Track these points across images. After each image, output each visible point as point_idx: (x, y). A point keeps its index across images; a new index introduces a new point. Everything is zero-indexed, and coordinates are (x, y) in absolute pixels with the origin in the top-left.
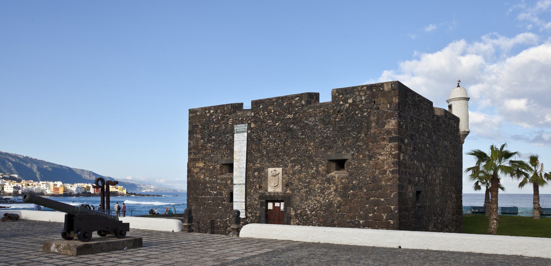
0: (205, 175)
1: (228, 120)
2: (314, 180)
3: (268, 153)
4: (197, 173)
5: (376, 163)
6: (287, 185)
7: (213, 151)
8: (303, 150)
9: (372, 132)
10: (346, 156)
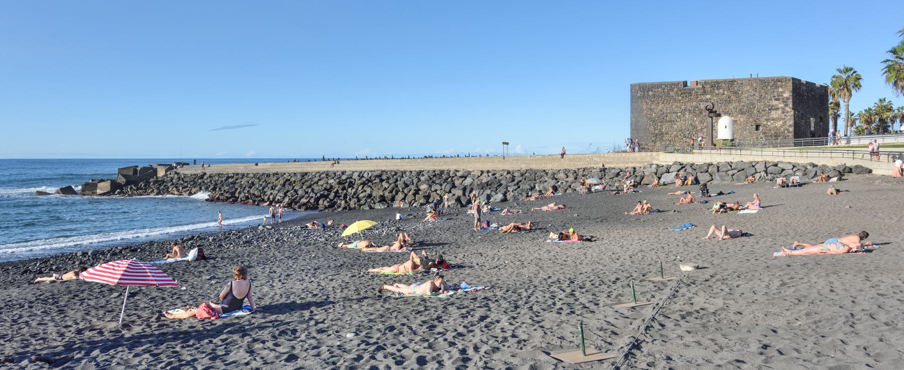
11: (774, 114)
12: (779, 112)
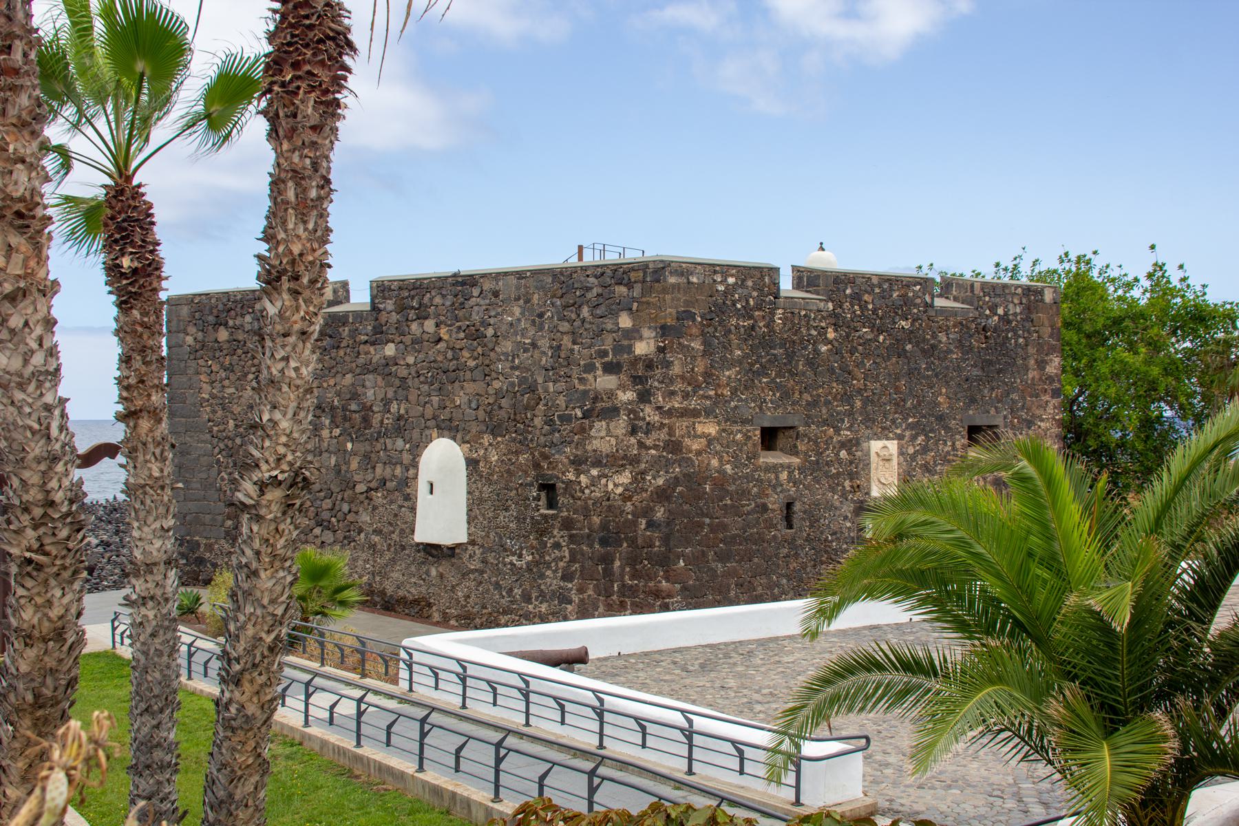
3: (864, 406)
4: (699, 453)
7: (734, 392)
8: (929, 403)
9: (1030, 376)
11: (605, 437)
12: (621, 425)
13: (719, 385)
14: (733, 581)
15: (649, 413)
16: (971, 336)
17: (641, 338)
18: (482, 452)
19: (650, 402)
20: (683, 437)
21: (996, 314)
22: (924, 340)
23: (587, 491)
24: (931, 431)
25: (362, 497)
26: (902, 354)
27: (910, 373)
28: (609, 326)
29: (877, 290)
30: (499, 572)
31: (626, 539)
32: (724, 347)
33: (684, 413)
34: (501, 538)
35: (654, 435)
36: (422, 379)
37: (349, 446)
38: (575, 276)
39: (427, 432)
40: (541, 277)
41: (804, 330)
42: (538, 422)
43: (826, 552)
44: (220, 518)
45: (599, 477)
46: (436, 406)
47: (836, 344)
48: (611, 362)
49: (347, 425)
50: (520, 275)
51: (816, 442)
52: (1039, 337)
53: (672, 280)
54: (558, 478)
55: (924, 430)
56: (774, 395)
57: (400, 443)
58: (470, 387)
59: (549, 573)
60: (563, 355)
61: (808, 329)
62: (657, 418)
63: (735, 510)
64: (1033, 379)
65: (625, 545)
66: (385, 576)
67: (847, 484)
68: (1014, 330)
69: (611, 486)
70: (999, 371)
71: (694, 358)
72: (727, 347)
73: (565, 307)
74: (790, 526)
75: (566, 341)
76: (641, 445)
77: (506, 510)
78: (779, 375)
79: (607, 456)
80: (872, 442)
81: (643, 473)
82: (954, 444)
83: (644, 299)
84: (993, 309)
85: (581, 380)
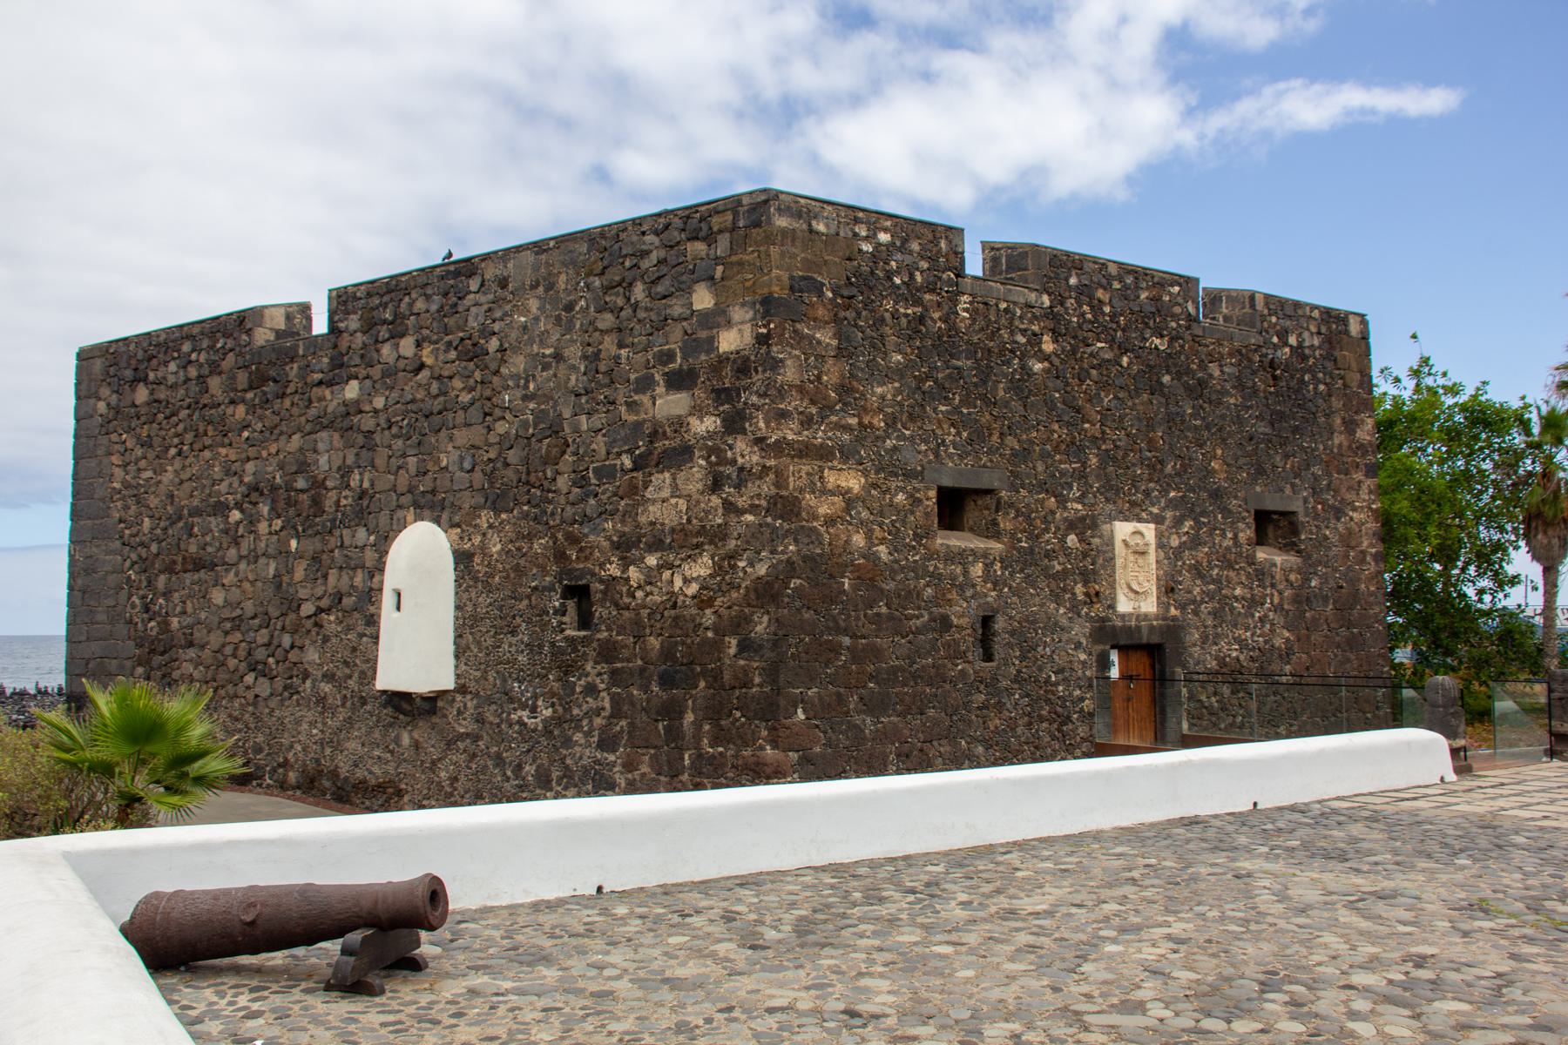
0: (869, 535)
1: (953, 299)
2: (1232, 574)
4: (830, 521)
5: (1350, 531)
6: (1168, 589)
7: (891, 422)
9: (1337, 442)
10: (1296, 502)
11: (667, 500)
12: (694, 476)
13: (864, 409)
14: (891, 749)
15: (743, 451)
16: (1254, 373)
17: (729, 324)
18: (477, 540)
19: (744, 432)
20: (801, 491)
21: (1286, 344)
22: (1189, 372)
23: (639, 594)
24: (1203, 513)
25: (309, 624)
26: (1156, 388)
27: (1170, 420)
28: (677, 310)
29: (1116, 285)
30: (501, 738)
31: (703, 674)
32: (873, 346)
33: (805, 451)
34: (505, 680)
35: (751, 488)
36: (395, 430)
37: (294, 543)
38: (623, 236)
39: (400, 513)
40: (571, 246)
41: (1004, 333)
42: (563, 482)
43: (1048, 701)
44: (129, 664)
45: (660, 567)
46: (413, 470)
47: (1056, 361)
48: (681, 370)
49: (292, 511)
50: (538, 247)
51: (1028, 518)
52: (1345, 386)
53: (782, 222)
54: (593, 574)
55: (1192, 510)
56: (959, 434)
57: (361, 533)
58: (462, 437)
59: (578, 737)
60: (602, 368)
61: (1012, 333)
62: (755, 458)
63: (896, 625)
64: (1340, 445)
65: (702, 684)
66: (338, 747)
67: (1079, 589)
68: (1310, 370)
69: (678, 583)
70: (1295, 430)
71: (821, 358)
72: (878, 344)
73: (607, 289)
74: (988, 657)
75: (609, 345)
76: (729, 507)
77: (513, 633)
78: (965, 402)
79: (673, 530)
80: (1117, 524)
81: (733, 556)
82: (1235, 537)
83: (734, 258)
84: (1283, 334)
85: (632, 406)
